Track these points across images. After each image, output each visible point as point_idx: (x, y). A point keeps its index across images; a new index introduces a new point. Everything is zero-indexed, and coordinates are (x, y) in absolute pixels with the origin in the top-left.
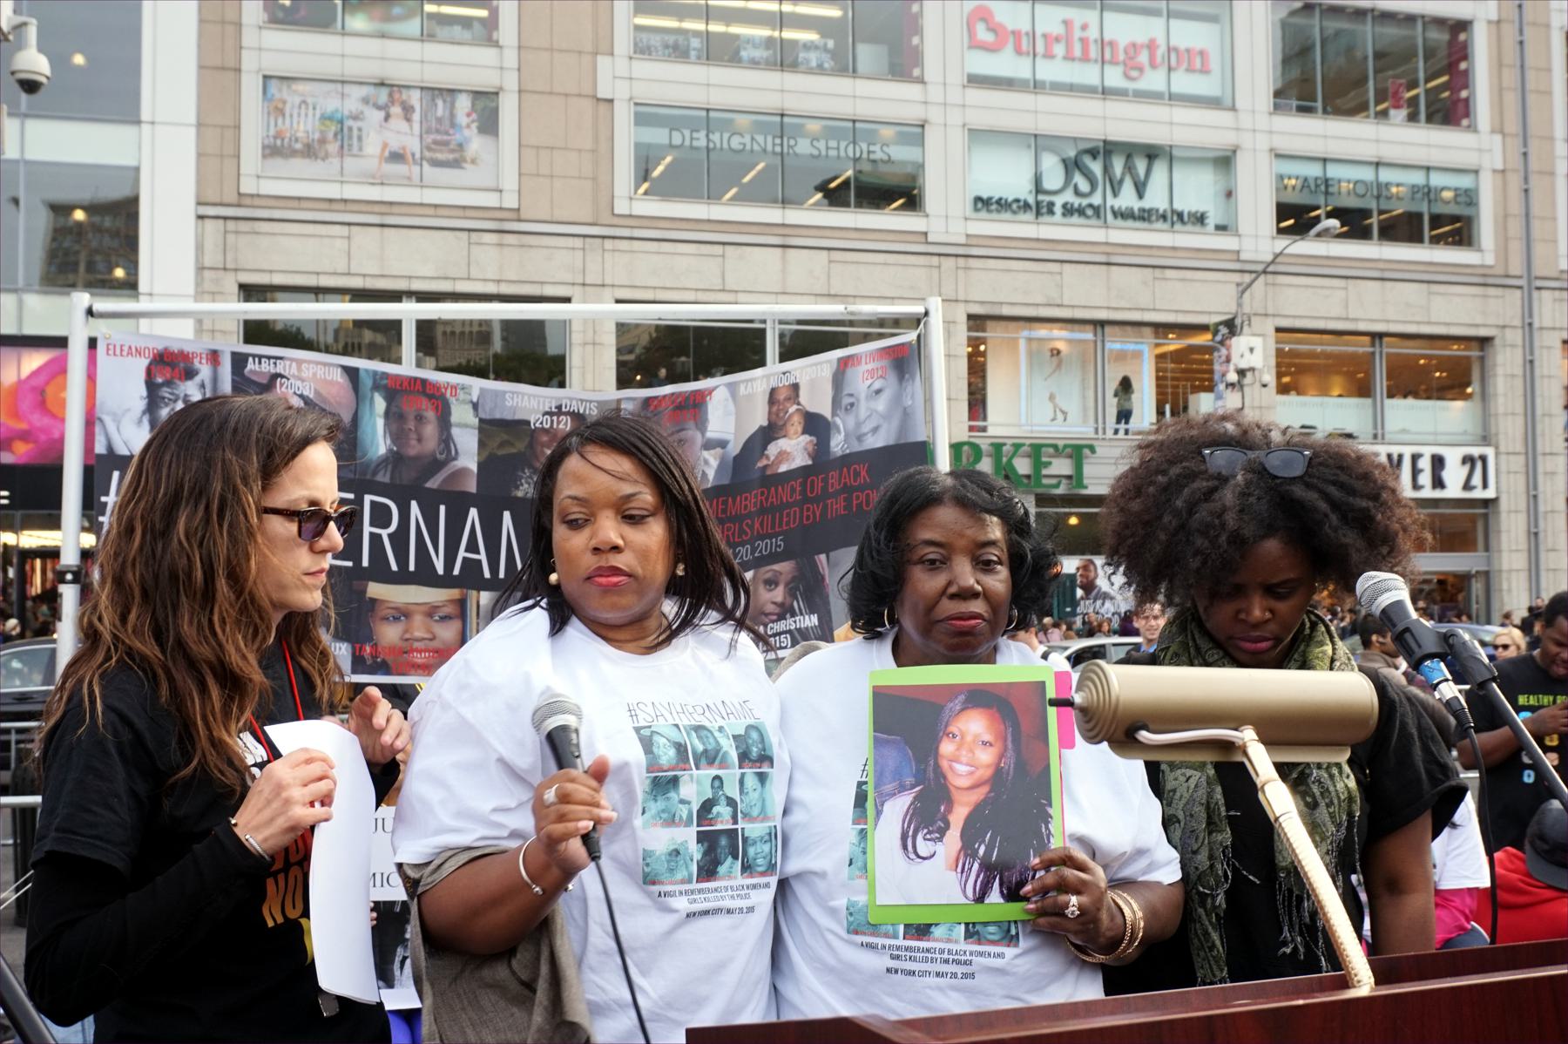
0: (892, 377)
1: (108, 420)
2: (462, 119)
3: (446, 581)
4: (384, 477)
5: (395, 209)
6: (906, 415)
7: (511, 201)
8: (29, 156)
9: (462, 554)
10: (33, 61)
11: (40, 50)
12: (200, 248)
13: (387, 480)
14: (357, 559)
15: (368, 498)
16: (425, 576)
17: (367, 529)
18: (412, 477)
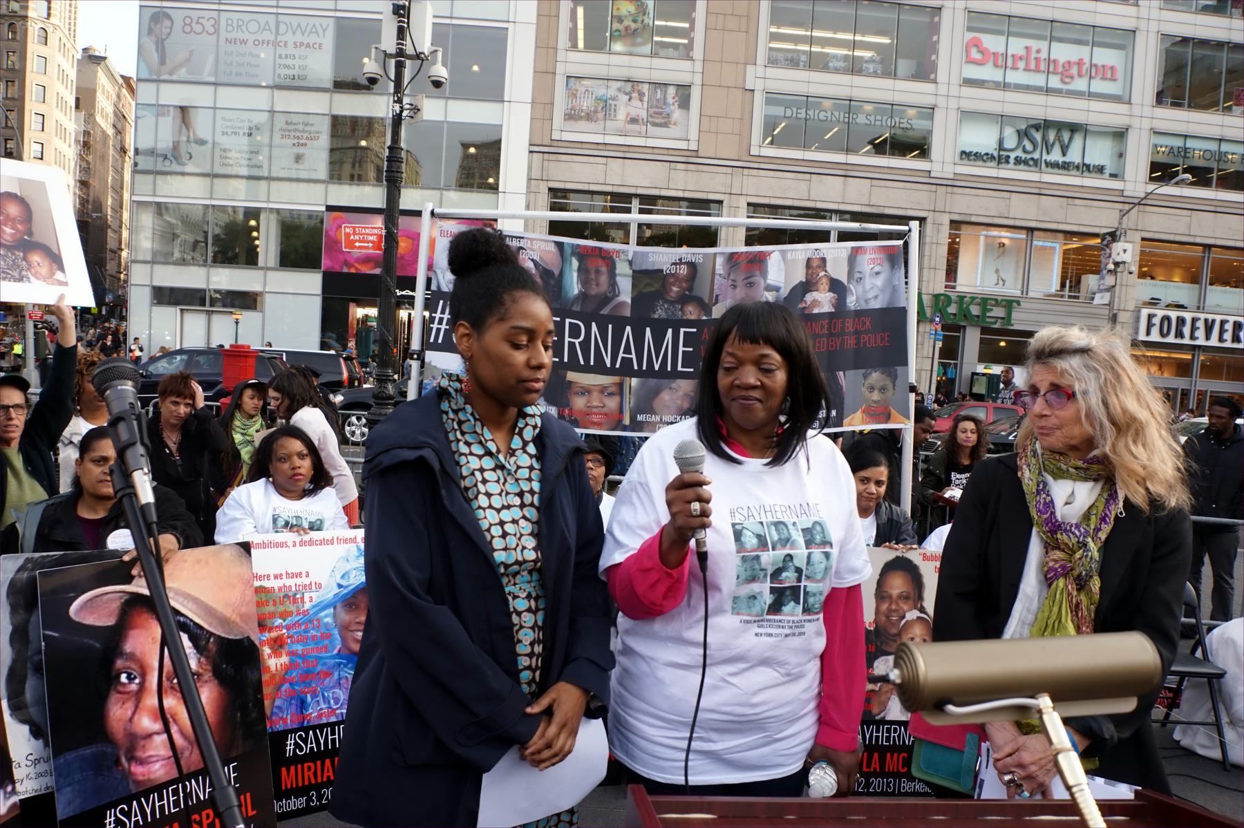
0: (887, 266)
1: (438, 272)
2: (670, 100)
3: (611, 372)
4: (577, 308)
5: (632, 149)
6: (894, 290)
7: (693, 147)
8: (452, 118)
9: (621, 355)
10: (440, 71)
11: (444, 64)
12: (530, 168)
13: (578, 309)
14: (562, 358)
15: (568, 321)
16: (600, 368)
17: (567, 339)
18: (594, 308)
